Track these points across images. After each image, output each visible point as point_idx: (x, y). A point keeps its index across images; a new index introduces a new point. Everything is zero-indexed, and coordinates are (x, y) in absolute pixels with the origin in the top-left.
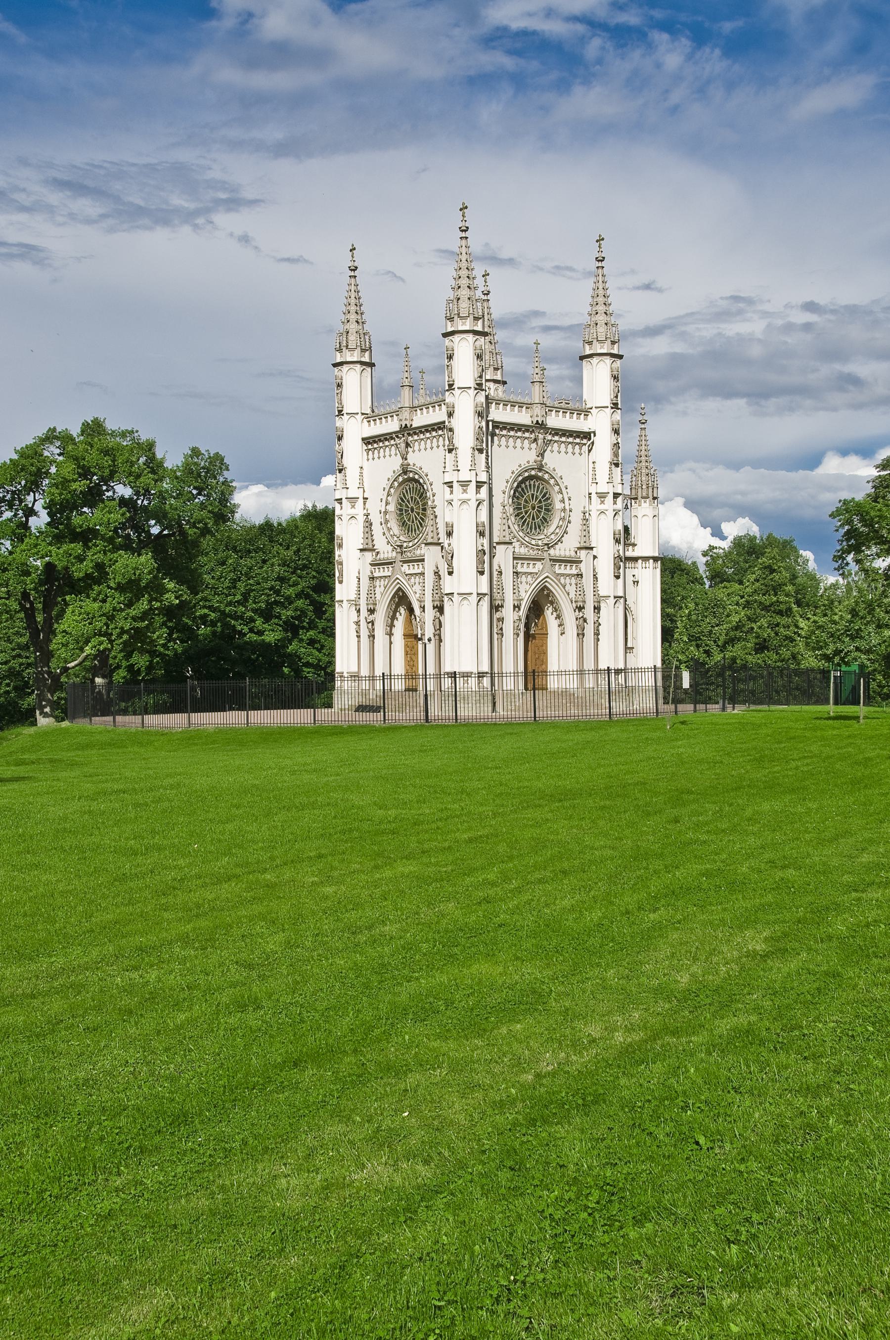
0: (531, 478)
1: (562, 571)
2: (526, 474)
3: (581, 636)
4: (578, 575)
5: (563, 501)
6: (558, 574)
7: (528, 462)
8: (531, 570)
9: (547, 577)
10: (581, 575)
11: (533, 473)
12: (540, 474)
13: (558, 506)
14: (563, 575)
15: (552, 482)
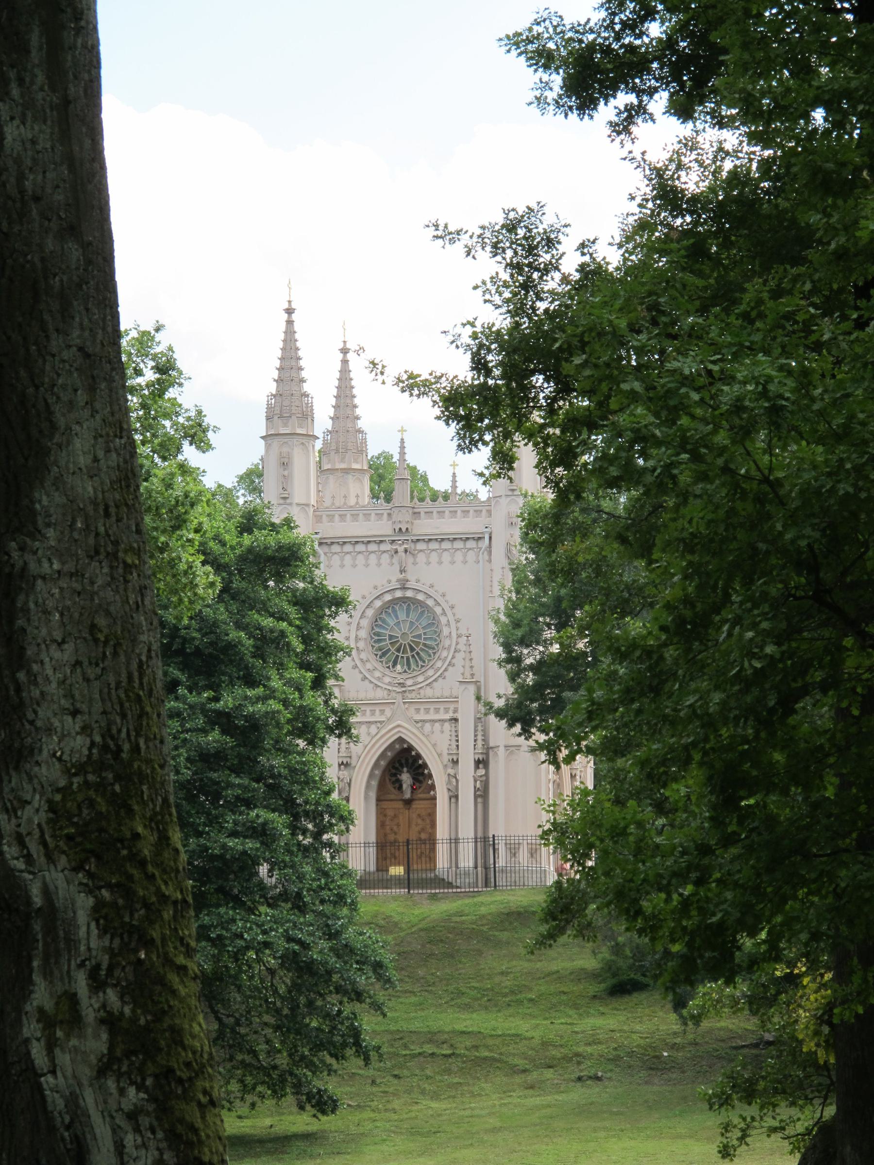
0: (395, 601)
1: (432, 716)
2: (388, 597)
3: (453, 800)
4: (451, 720)
5: (448, 624)
6: (417, 722)
7: (389, 582)
8: (378, 717)
9: (398, 726)
10: (456, 720)
11: (399, 594)
12: (409, 594)
13: (446, 631)
14: (434, 721)
15: (430, 602)
